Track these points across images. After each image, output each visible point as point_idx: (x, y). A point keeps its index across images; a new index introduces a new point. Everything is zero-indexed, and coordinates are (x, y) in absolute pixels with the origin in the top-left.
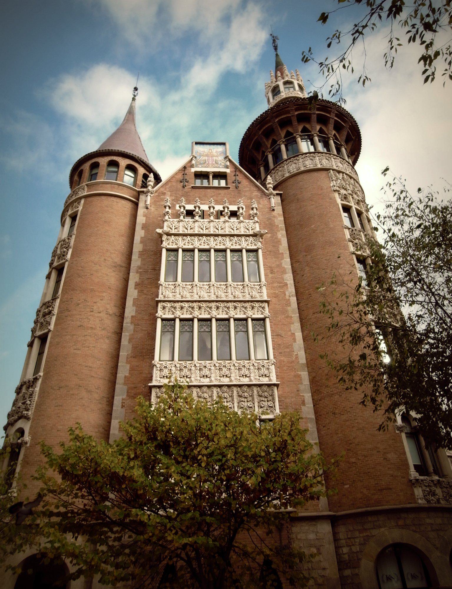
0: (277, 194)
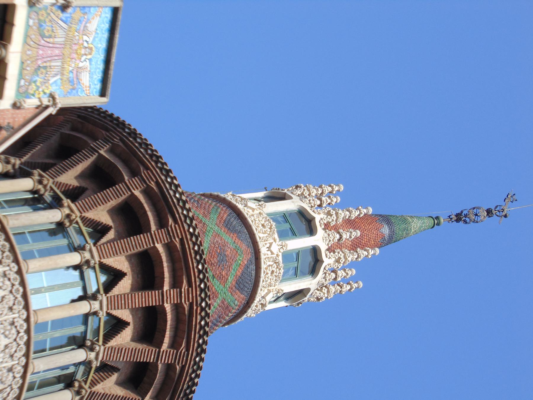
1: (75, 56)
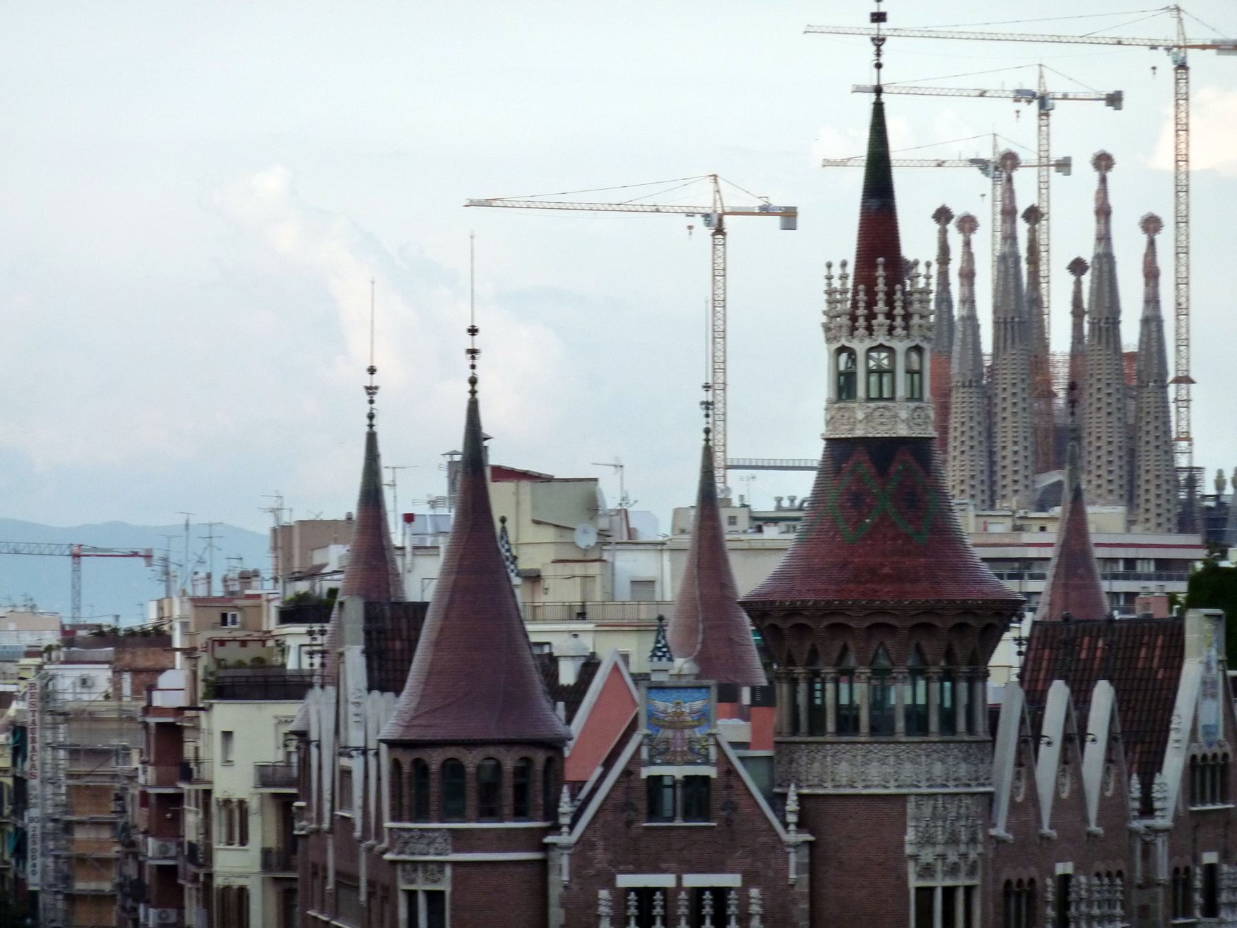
0: (804, 842)
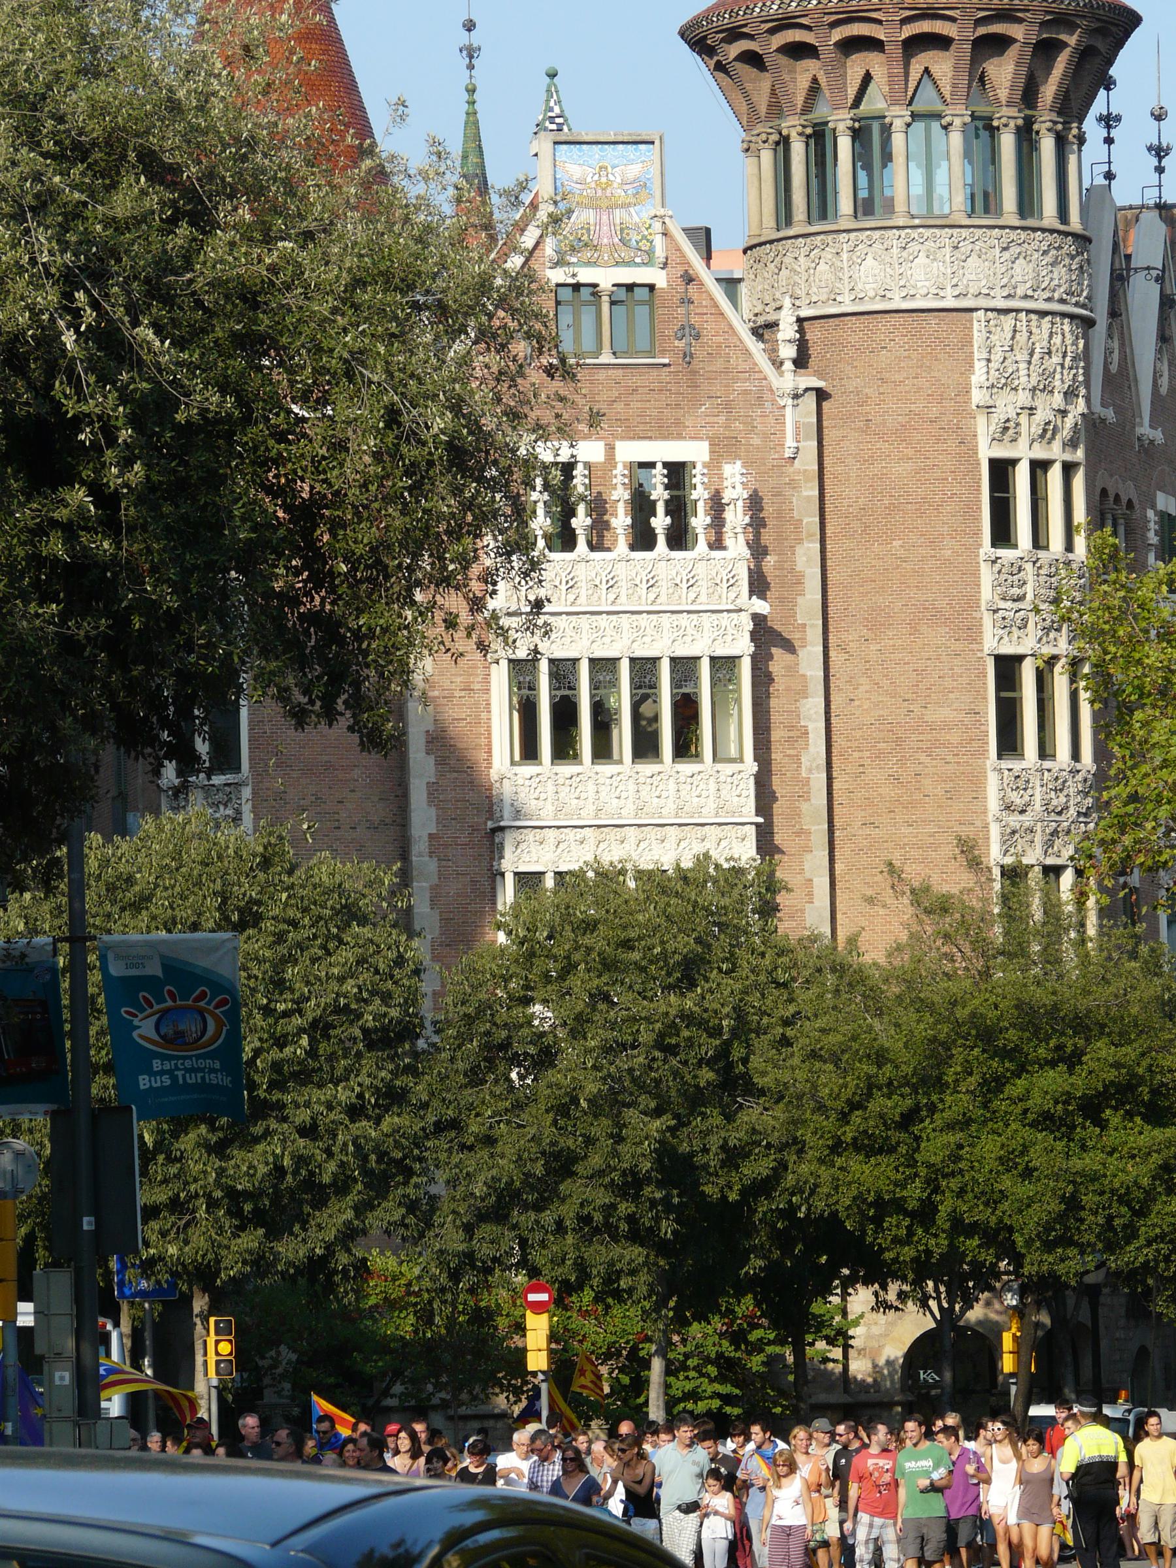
0: (807, 390)
1: (608, 193)
